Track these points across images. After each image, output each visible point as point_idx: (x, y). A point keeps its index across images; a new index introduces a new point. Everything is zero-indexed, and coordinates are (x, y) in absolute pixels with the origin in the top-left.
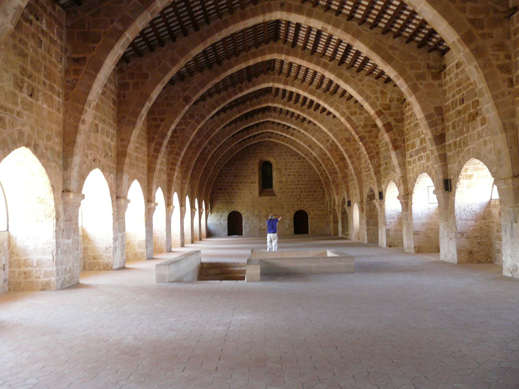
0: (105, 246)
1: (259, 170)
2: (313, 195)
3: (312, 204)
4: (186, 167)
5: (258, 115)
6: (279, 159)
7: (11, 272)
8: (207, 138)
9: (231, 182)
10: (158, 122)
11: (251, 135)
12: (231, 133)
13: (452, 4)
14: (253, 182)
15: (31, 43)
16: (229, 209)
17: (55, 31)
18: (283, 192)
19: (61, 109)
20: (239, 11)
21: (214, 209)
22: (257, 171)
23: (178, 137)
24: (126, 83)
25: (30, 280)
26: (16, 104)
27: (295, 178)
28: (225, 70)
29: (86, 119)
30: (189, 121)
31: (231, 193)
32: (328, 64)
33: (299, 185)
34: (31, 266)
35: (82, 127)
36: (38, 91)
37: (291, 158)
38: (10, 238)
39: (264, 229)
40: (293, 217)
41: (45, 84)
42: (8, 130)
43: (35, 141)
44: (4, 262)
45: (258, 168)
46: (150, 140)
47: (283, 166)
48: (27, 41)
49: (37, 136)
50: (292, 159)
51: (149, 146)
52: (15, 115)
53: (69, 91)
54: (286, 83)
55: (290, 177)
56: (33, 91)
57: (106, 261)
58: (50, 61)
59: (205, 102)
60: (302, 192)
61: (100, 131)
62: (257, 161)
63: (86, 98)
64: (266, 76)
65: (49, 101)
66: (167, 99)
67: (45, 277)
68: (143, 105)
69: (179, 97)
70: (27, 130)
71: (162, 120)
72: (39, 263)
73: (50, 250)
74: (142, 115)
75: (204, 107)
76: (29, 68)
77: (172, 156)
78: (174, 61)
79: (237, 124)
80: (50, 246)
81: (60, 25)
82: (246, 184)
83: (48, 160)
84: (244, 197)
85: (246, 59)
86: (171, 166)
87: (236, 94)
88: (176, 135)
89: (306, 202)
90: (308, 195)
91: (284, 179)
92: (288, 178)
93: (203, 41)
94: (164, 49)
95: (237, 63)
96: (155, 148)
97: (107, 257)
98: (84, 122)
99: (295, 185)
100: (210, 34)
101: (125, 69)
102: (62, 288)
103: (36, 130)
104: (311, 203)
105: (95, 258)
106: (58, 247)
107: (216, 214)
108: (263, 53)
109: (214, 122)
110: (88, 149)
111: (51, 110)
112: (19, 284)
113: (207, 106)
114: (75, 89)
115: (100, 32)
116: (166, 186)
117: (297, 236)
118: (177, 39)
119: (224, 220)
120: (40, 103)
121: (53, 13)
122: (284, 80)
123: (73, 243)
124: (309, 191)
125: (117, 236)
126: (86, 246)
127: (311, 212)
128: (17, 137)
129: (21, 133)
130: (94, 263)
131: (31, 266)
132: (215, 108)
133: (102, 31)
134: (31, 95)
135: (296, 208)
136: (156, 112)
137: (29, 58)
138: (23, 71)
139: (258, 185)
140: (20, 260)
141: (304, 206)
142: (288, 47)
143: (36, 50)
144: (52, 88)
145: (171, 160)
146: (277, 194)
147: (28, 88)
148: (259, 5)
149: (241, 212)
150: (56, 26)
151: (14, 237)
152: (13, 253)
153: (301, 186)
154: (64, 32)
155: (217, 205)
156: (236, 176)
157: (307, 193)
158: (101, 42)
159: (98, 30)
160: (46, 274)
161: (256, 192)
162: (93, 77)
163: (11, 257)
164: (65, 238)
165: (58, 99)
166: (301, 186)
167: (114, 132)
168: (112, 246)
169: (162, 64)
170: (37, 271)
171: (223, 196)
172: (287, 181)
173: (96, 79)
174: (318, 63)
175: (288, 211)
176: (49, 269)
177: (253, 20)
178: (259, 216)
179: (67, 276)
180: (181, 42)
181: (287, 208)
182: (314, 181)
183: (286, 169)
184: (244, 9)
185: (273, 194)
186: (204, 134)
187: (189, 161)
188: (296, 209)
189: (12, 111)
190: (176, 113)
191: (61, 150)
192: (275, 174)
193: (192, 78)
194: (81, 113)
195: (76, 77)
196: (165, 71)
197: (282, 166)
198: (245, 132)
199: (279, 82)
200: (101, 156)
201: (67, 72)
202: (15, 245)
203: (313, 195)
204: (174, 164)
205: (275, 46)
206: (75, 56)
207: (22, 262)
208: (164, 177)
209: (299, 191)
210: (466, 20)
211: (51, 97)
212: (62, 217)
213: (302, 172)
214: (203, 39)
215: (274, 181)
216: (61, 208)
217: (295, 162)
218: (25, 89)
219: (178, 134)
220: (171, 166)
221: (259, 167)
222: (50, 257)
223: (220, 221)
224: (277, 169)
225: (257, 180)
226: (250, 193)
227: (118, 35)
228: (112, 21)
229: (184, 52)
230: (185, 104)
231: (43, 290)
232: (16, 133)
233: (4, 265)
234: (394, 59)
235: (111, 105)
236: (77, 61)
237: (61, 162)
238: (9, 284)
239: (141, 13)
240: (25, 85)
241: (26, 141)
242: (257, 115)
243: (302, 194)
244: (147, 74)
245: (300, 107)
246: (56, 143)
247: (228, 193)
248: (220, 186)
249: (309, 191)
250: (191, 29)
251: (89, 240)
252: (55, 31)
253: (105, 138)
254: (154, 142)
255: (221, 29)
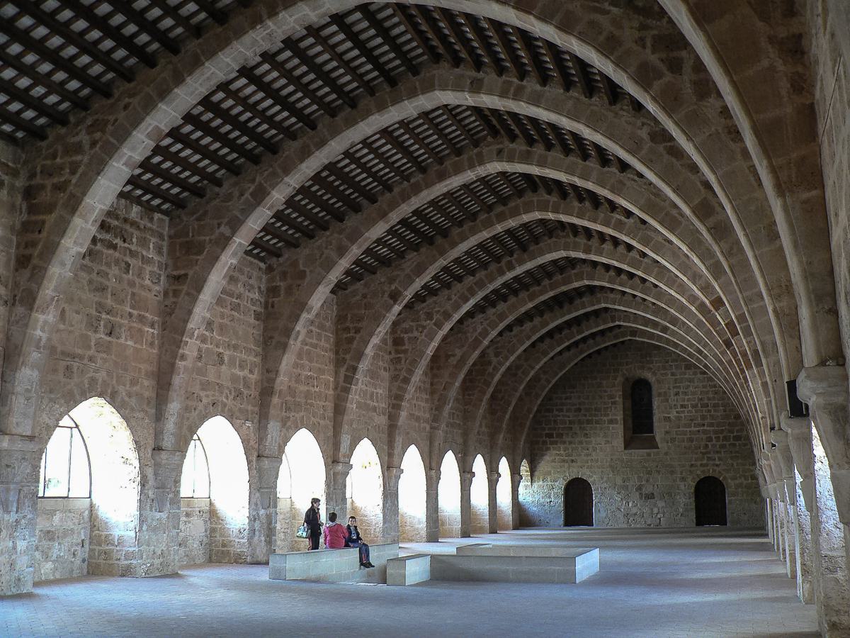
0: (237, 527)
1: (624, 397)
2: (734, 445)
3: (733, 464)
4: (439, 400)
5: (584, 299)
6: (662, 374)
7: (91, 550)
8: (475, 349)
9: (571, 422)
10: (351, 334)
11: (587, 333)
12: (534, 333)
13: (678, 161)
14: (611, 422)
15: (114, 271)
16: (568, 474)
17: (151, 246)
18: (673, 440)
19: (156, 342)
20: (435, 169)
21: (536, 473)
22: (619, 399)
23: (405, 351)
24: (276, 286)
25: (111, 562)
26: (89, 347)
27: (696, 412)
28: (454, 245)
29: (187, 352)
30: (424, 323)
31: (570, 443)
32: (626, 223)
33: (704, 425)
34: (113, 545)
35: (180, 364)
36: (120, 326)
37: (687, 371)
38: (92, 506)
39: (635, 514)
40: (693, 490)
41: (131, 315)
42: (76, 380)
43: (113, 388)
44: (83, 538)
45: (621, 393)
46: (339, 362)
47: (671, 388)
48: (108, 271)
49: (117, 381)
50: (689, 374)
51: (336, 373)
52: (86, 361)
53: (167, 319)
54: (587, 251)
55: (686, 410)
56: (113, 327)
57: (239, 550)
58: (142, 286)
59: (450, 291)
60: (710, 439)
61: (226, 361)
62: (620, 379)
63: (186, 327)
64: (554, 239)
65: (137, 335)
66: (364, 296)
67: (126, 559)
68: (297, 318)
69: (383, 293)
70: (101, 376)
71: (357, 331)
72: (121, 541)
73: (132, 525)
74: (299, 332)
75: (449, 299)
76: (109, 302)
77: (397, 383)
78: (342, 251)
79: (545, 317)
80: (133, 519)
81: (161, 237)
82: (598, 425)
83: (132, 409)
84: (595, 449)
85: (488, 224)
86: (394, 402)
87: (502, 273)
88: (403, 348)
89: (720, 459)
90: (723, 446)
91: (673, 415)
92: (683, 412)
93: (383, 217)
94: (328, 233)
95: (474, 231)
96: (345, 375)
97: (240, 544)
98: (183, 357)
99: (694, 427)
100: (393, 206)
101: (275, 266)
102: (147, 576)
103: (114, 374)
104: (730, 462)
105: (224, 545)
106: (142, 520)
107: (541, 483)
108: (515, 213)
109: (486, 320)
110: (203, 389)
111: (139, 347)
112: (98, 565)
113: (454, 298)
114: (174, 315)
115: (205, 240)
116: (385, 437)
117: (701, 528)
118: (347, 217)
119: (557, 496)
120: (122, 341)
121: (149, 225)
122: (585, 244)
123: (168, 518)
124: (725, 438)
125: (258, 514)
126: (213, 526)
127: (729, 481)
128: (87, 386)
129: (93, 381)
130: (223, 551)
131: (113, 545)
132: (467, 300)
133: (208, 238)
134: (110, 334)
135: (699, 472)
136: (349, 319)
137: (110, 290)
138: (101, 307)
139: (622, 426)
140: (100, 536)
141: (715, 468)
142: (556, 200)
143: (121, 277)
144: (141, 319)
145: (394, 391)
146: (660, 446)
147: (105, 326)
148: (465, 156)
149: (590, 481)
150: (153, 240)
151: (97, 507)
152: (95, 526)
153: (708, 428)
154: (165, 244)
155: (543, 466)
156: (580, 410)
157: (721, 443)
158: (205, 253)
159: (203, 238)
160: (128, 556)
161: (619, 442)
162: (194, 300)
163: (92, 531)
164: (156, 510)
165: (152, 331)
166: (708, 428)
167: (258, 360)
168: (247, 527)
169: (324, 256)
170: (117, 551)
171: (554, 449)
172: (679, 418)
173: (198, 302)
174: (607, 224)
175: (683, 479)
176: (131, 549)
177: (457, 179)
178: (626, 488)
179: (157, 562)
180: (352, 221)
181: (681, 473)
182: (735, 418)
183: (677, 394)
184: (442, 164)
185: (652, 444)
186: (470, 340)
187: (444, 388)
188: (700, 473)
189: (81, 357)
190: (378, 319)
191: (154, 395)
192: (656, 403)
193: (403, 261)
194: (179, 347)
195: (174, 300)
196: (329, 266)
197: (669, 389)
198: (574, 329)
199: (575, 249)
200: (227, 399)
201: (166, 294)
202: (97, 517)
203: (734, 445)
204: (399, 398)
205: (535, 199)
206: (175, 273)
207: (103, 538)
208: (382, 420)
209: (704, 437)
210: (699, 184)
211: (140, 330)
212: (151, 482)
213: (709, 399)
214: (383, 215)
215: (654, 418)
216: (150, 472)
217: (696, 380)
218: (102, 328)
219: (407, 347)
220: (394, 402)
221: (624, 391)
222: (132, 534)
223: (550, 497)
224: (659, 395)
225: (620, 417)
226: (607, 442)
227: (224, 242)
228: (219, 225)
229: (354, 237)
230: (392, 302)
231: (123, 576)
232: (86, 381)
233: (83, 541)
234: (680, 223)
235: (252, 321)
236: (178, 279)
237: (153, 411)
238: (89, 564)
239: (253, 211)
240: (102, 323)
241: (99, 390)
242: (581, 298)
243: (709, 443)
244: (305, 272)
245: (642, 285)
246: (147, 387)
247: (565, 443)
248: (550, 429)
249: (725, 438)
250: (365, 202)
251: (218, 518)
252: (151, 246)
253: (237, 372)
254: (346, 366)
255: (409, 198)
